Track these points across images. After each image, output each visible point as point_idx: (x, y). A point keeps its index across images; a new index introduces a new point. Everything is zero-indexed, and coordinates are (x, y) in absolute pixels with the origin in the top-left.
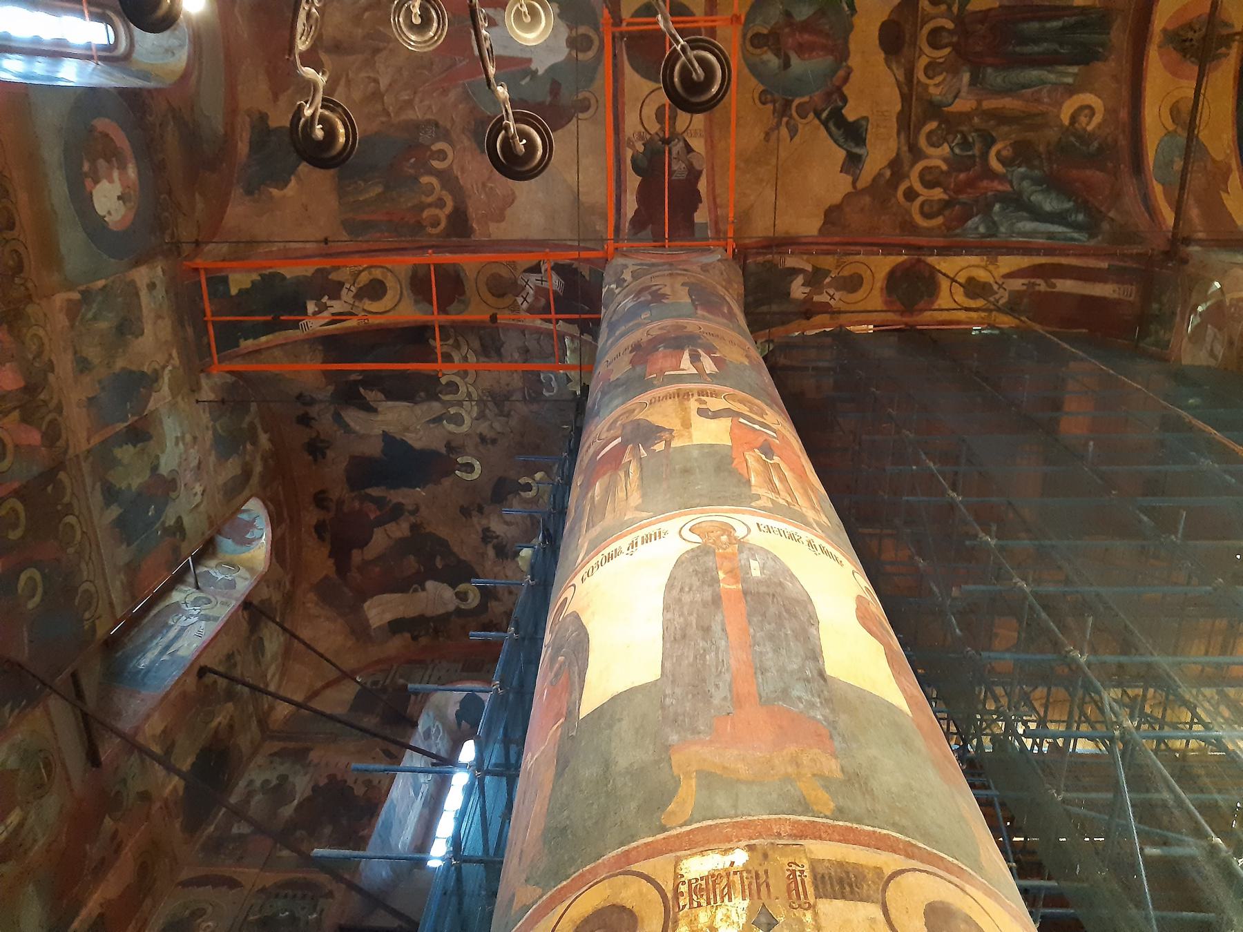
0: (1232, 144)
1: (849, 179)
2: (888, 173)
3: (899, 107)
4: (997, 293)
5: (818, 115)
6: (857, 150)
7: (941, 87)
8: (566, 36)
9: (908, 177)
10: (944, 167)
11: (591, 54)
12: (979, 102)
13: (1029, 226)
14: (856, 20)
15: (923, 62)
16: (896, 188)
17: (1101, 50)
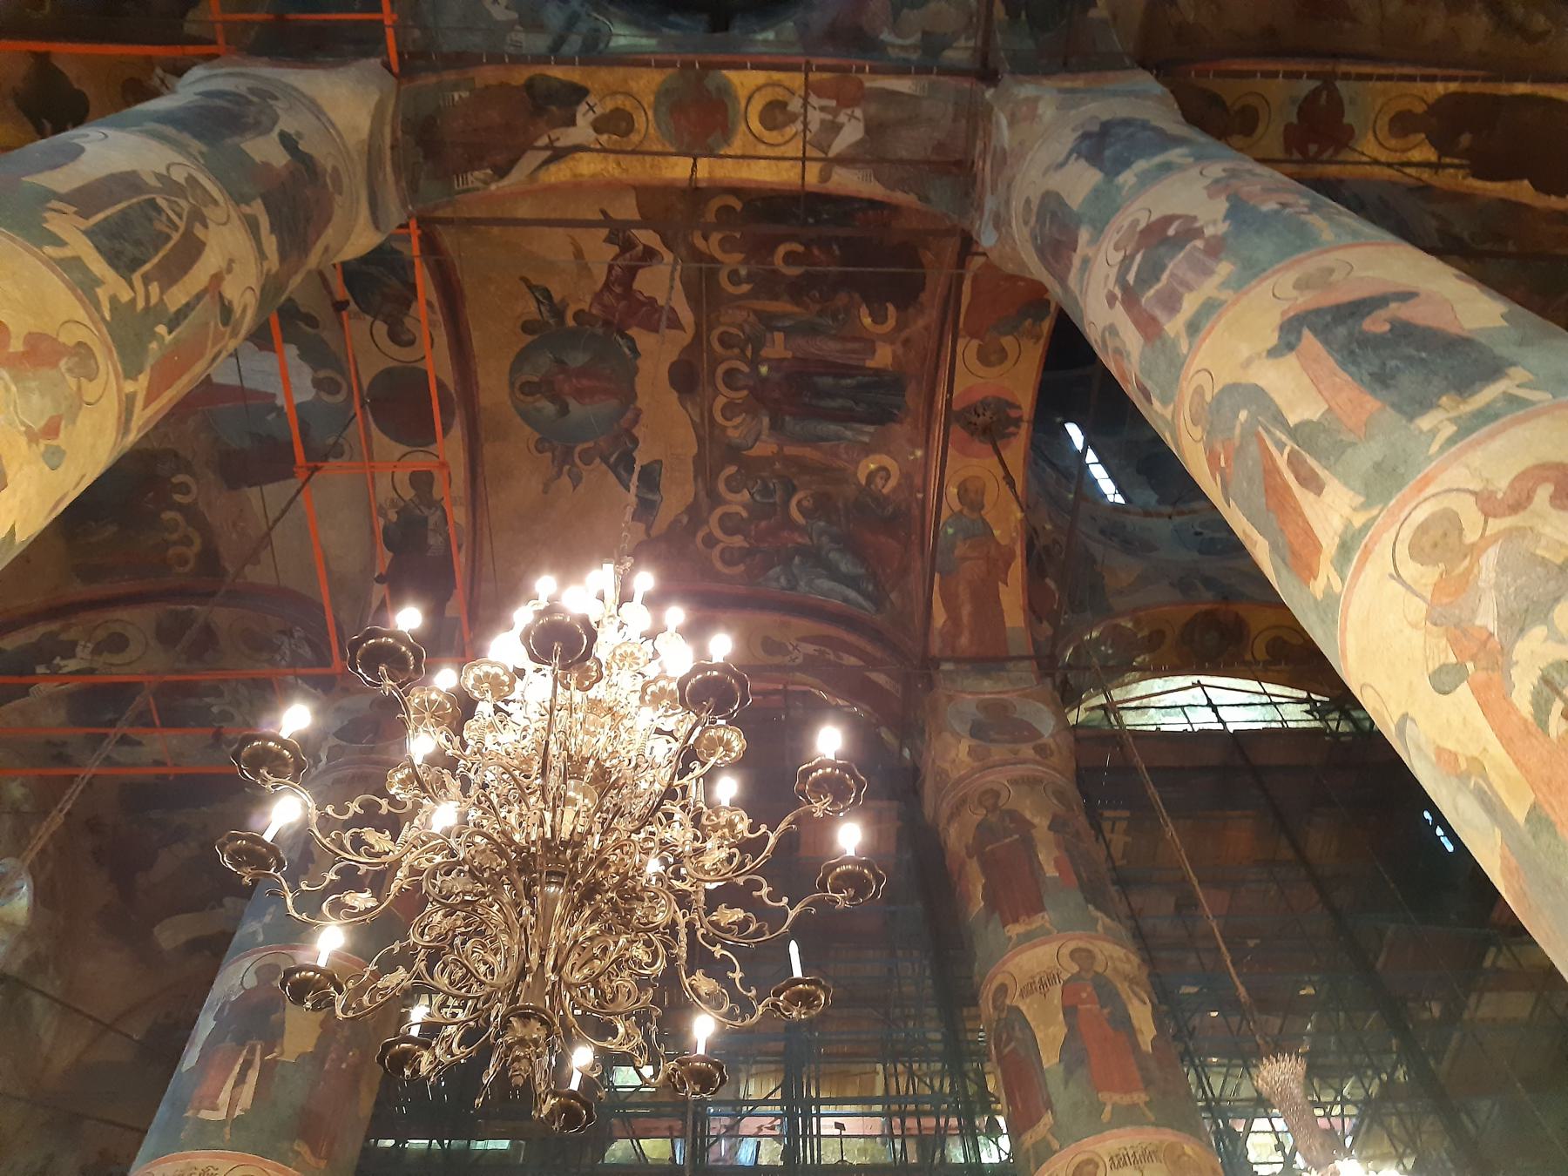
0: (1019, 527)
1: (641, 526)
2: (685, 520)
3: (695, 450)
4: (791, 653)
5: (605, 460)
6: (650, 496)
7: (741, 428)
8: (311, 377)
9: (708, 522)
10: (745, 514)
11: (340, 398)
12: (781, 449)
13: (826, 584)
14: (640, 362)
15: (720, 401)
16: (694, 535)
17: (896, 411)
